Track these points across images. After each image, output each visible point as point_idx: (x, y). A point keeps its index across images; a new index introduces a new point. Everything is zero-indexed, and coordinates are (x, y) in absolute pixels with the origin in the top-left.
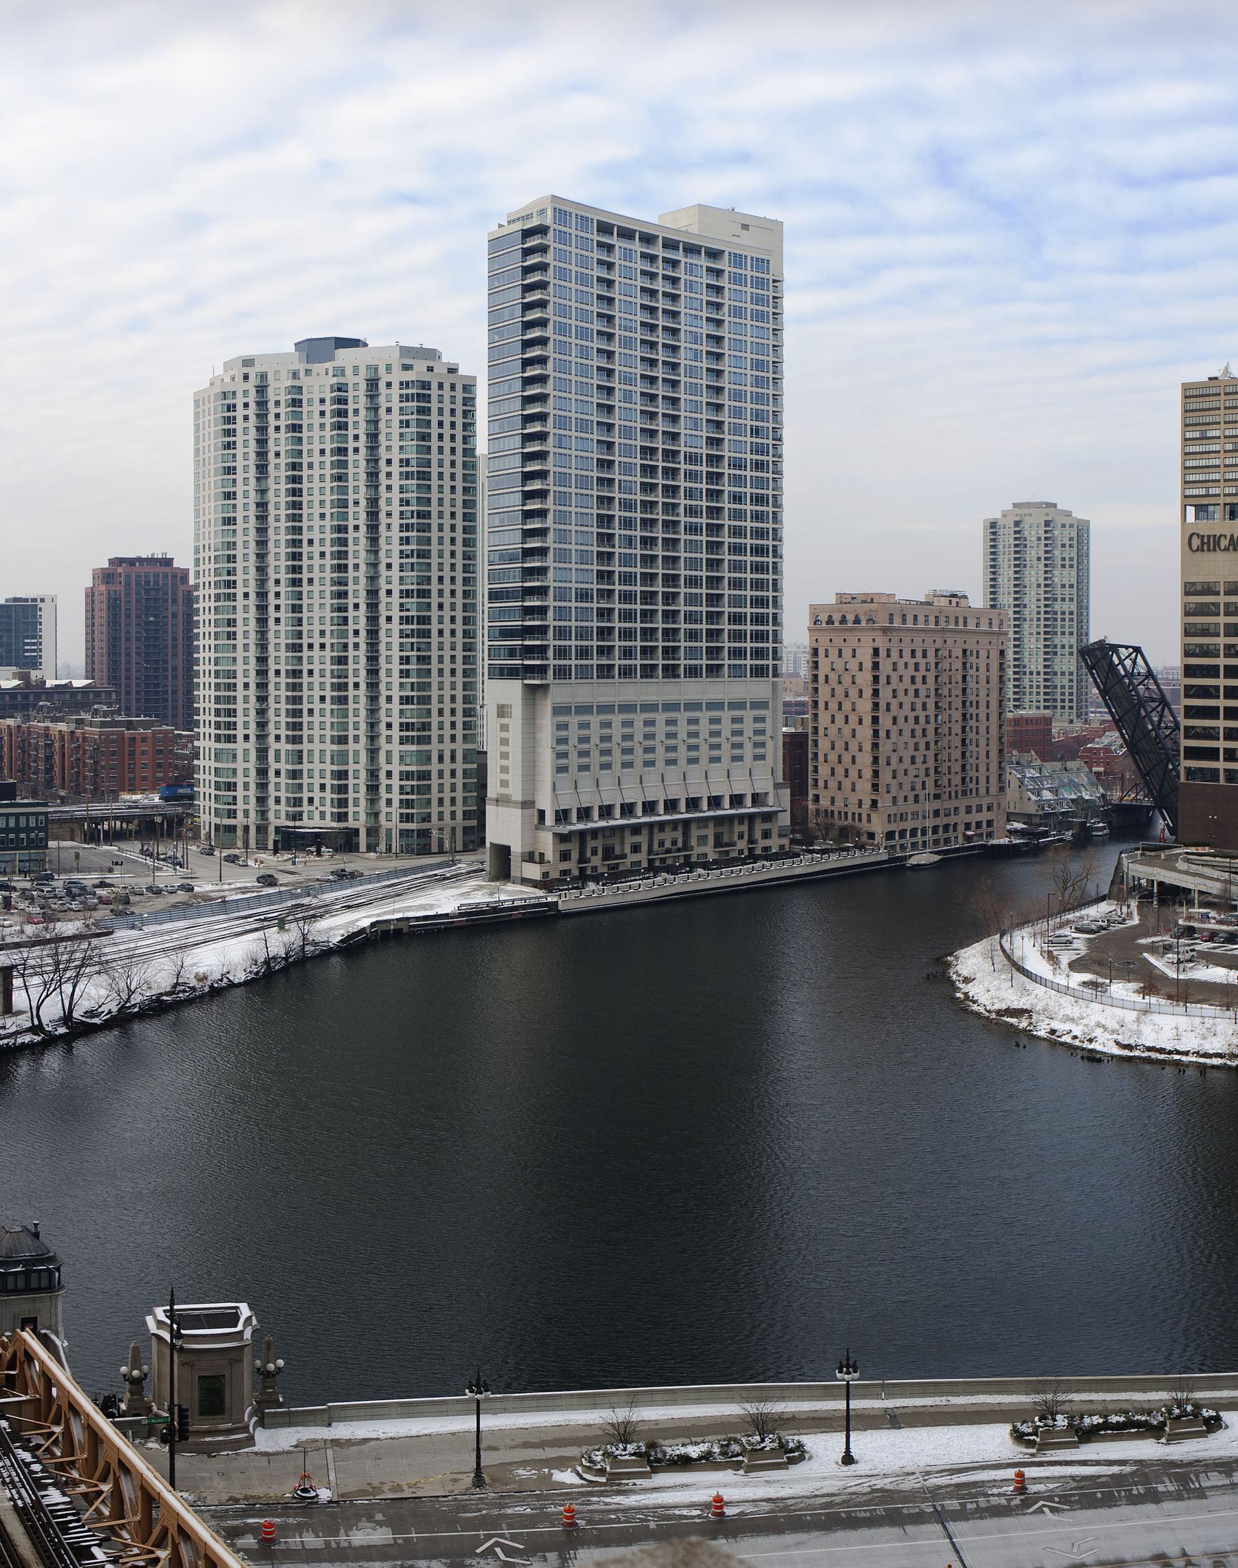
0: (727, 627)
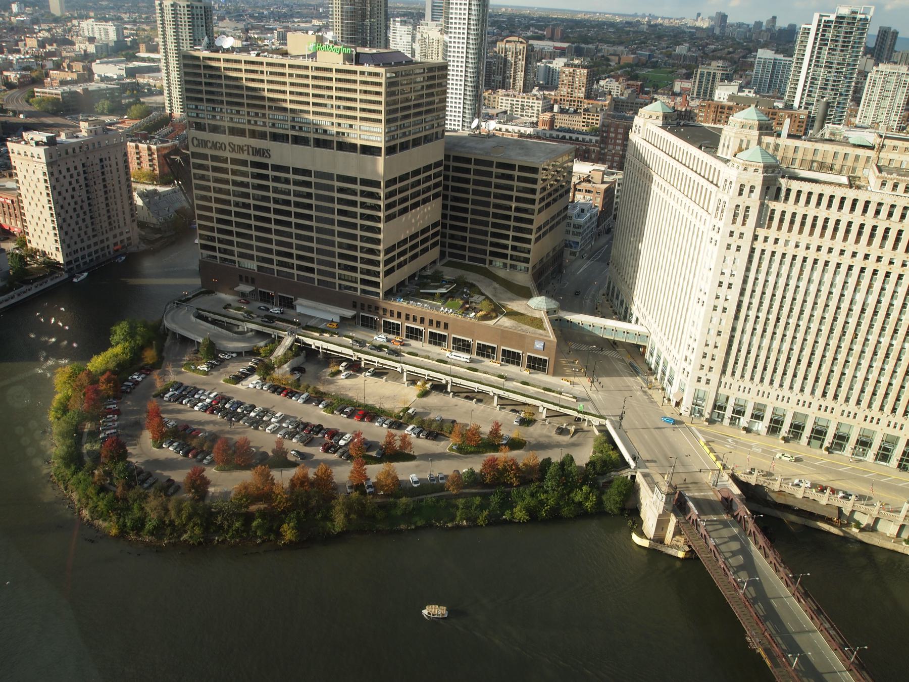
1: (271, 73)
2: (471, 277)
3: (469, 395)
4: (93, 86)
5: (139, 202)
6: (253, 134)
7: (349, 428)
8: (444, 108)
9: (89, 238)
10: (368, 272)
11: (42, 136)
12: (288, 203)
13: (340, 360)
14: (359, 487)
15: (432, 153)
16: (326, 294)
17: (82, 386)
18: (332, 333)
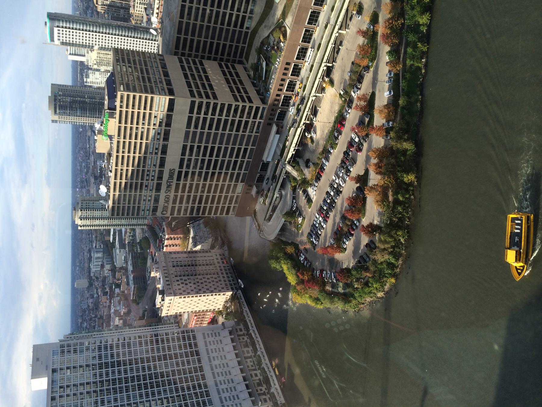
0: (173, 352)
1: (122, 164)
2: (257, 43)
3: (336, 50)
4: (130, 268)
5: (199, 248)
6: (160, 178)
7: (348, 133)
8: (144, 53)
9: (219, 277)
10: (249, 114)
11: (159, 298)
12: (203, 161)
13: (303, 137)
14: (388, 131)
15: (174, 66)
16: (261, 143)
17: (305, 289)
18: (286, 140)
